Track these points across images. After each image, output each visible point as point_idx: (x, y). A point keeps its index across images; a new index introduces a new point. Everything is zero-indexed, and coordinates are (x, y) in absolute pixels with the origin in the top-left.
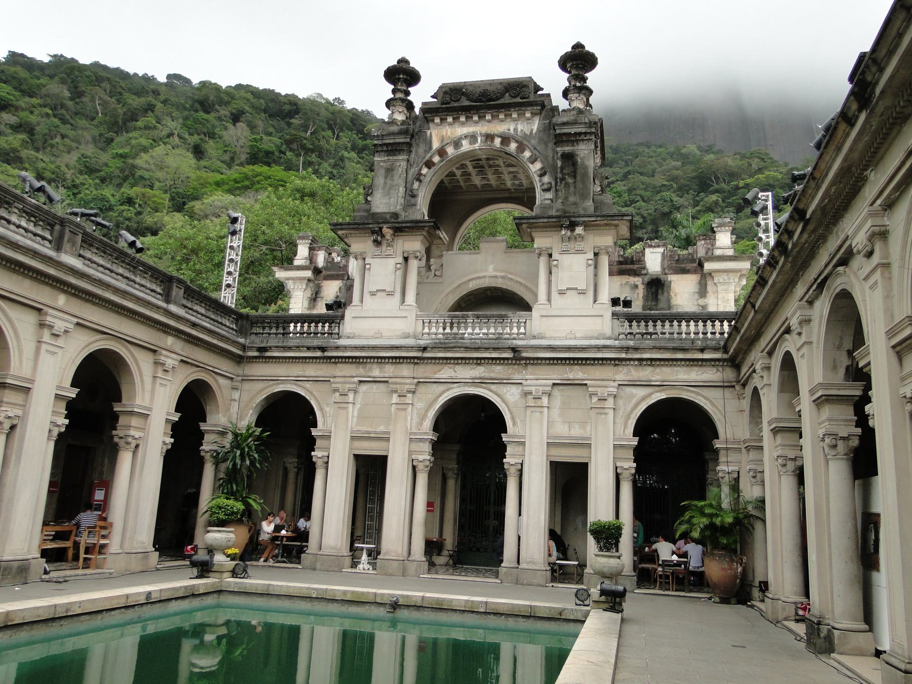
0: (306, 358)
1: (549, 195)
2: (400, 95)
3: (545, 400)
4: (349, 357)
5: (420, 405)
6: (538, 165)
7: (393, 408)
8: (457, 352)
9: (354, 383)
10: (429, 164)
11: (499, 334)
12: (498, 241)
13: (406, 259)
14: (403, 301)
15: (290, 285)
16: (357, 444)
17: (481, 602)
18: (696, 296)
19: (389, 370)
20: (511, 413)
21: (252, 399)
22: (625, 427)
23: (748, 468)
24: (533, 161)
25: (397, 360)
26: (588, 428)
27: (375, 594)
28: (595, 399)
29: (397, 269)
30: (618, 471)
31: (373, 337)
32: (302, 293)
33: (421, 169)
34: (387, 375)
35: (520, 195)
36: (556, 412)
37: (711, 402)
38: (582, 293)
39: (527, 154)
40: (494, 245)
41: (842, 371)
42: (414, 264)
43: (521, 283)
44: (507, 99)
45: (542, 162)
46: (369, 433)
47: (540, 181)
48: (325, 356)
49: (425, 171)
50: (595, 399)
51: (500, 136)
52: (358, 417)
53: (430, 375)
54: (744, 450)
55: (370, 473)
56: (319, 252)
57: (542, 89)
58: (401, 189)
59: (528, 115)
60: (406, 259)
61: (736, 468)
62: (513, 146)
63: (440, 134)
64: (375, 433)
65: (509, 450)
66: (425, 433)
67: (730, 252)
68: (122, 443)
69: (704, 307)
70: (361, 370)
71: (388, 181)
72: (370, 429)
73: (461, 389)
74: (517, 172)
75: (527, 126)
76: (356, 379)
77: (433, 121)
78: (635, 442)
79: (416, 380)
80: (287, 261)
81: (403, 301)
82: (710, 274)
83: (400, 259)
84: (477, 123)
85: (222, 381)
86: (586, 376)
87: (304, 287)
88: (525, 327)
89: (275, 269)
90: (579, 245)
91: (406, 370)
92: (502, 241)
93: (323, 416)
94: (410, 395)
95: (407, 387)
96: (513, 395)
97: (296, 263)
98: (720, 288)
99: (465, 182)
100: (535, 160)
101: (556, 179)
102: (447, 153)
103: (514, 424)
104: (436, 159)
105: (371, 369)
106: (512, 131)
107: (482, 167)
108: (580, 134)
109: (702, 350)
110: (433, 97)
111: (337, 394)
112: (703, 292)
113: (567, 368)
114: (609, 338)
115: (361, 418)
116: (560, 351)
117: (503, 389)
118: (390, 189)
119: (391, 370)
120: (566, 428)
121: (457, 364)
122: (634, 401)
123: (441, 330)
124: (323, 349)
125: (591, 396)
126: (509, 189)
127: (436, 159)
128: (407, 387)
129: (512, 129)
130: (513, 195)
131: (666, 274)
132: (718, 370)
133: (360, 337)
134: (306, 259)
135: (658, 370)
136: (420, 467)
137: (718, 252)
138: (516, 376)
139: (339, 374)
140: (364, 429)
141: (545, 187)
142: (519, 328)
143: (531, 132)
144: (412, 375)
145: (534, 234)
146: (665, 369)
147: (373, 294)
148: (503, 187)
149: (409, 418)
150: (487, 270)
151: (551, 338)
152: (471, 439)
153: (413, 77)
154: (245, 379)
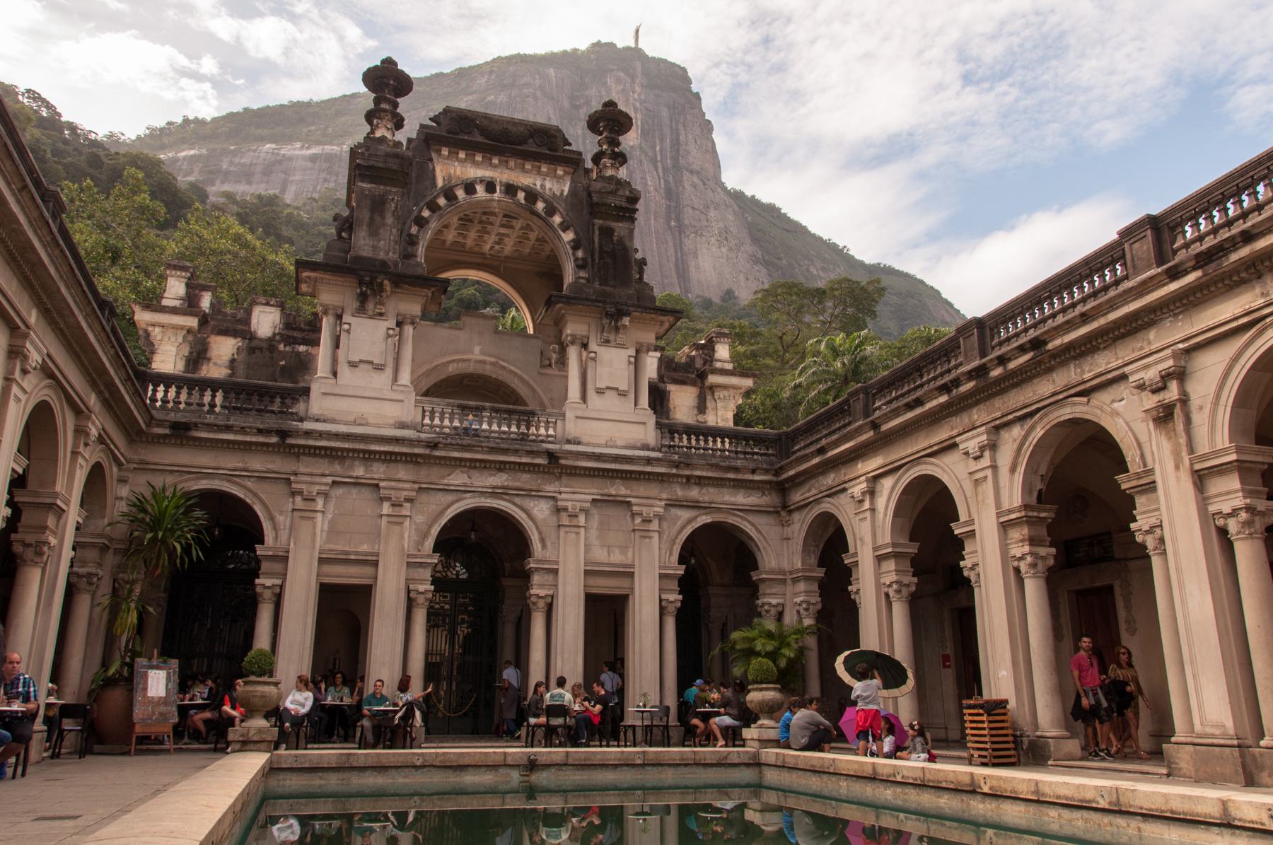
0: (251, 443)
1: (582, 274)
3: (582, 519)
4: (320, 448)
5: (420, 519)
7: (384, 519)
8: (477, 452)
9: (326, 484)
10: (433, 207)
11: (523, 434)
12: (485, 317)
14: (395, 379)
15: (156, 333)
16: (327, 569)
17: (638, 753)
20: (540, 533)
22: (671, 554)
23: (798, 600)
25: (390, 458)
26: (630, 554)
27: (505, 753)
28: (638, 520)
29: (389, 336)
31: (355, 423)
32: (174, 349)
33: (421, 211)
34: (376, 476)
36: (593, 533)
37: (749, 526)
38: (623, 394)
39: (557, 219)
40: (481, 321)
41: (1035, 494)
42: (409, 330)
43: (516, 374)
44: (531, 147)
45: (576, 233)
46: (347, 553)
47: (574, 254)
48: (285, 442)
49: (426, 213)
50: (638, 520)
51: (524, 190)
52: (329, 532)
53: (434, 479)
54: (789, 581)
55: (344, 611)
56: (204, 293)
58: (394, 231)
59: (560, 172)
60: (399, 324)
61: (781, 601)
62: (540, 206)
63: (450, 169)
64: (356, 553)
65: (536, 579)
66: (428, 556)
67: (729, 366)
68: (30, 553)
70: (337, 468)
71: (378, 219)
73: (477, 500)
74: (508, 236)
76: (329, 480)
77: (439, 152)
79: (416, 486)
80: (152, 302)
81: (395, 379)
82: (712, 388)
83: (392, 323)
84: (495, 166)
85: (115, 469)
86: (628, 492)
87: (180, 340)
89: (137, 309)
90: (621, 338)
91: (402, 472)
93: (275, 528)
94: (408, 505)
95: (405, 493)
96: (541, 510)
97: (165, 302)
98: (720, 404)
101: (592, 255)
102: (456, 198)
103: (544, 546)
104: (442, 201)
105: (351, 467)
106: (538, 187)
107: (471, 221)
108: (621, 207)
109: (753, 472)
111: (298, 499)
112: (701, 408)
114: (653, 450)
115: (333, 532)
116: (605, 461)
117: (530, 504)
120: (605, 553)
121: (475, 467)
122: (679, 523)
123: (447, 422)
124: (283, 434)
125: (633, 515)
127: (442, 201)
128: (405, 493)
129: (538, 183)
130: (487, 262)
134: (182, 299)
135: (704, 491)
136: (421, 599)
137: (718, 365)
139: (302, 469)
140: (340, 548)
141: (580, 262)
144: (411, 478)
145: (568, 317)
146: (711, 490)
147: (353, 365)
148: (476, 249)
149: (406, 535)
150: (472, 352)
151: (588, 444)
152: (483, 568)
154: (143, 467)
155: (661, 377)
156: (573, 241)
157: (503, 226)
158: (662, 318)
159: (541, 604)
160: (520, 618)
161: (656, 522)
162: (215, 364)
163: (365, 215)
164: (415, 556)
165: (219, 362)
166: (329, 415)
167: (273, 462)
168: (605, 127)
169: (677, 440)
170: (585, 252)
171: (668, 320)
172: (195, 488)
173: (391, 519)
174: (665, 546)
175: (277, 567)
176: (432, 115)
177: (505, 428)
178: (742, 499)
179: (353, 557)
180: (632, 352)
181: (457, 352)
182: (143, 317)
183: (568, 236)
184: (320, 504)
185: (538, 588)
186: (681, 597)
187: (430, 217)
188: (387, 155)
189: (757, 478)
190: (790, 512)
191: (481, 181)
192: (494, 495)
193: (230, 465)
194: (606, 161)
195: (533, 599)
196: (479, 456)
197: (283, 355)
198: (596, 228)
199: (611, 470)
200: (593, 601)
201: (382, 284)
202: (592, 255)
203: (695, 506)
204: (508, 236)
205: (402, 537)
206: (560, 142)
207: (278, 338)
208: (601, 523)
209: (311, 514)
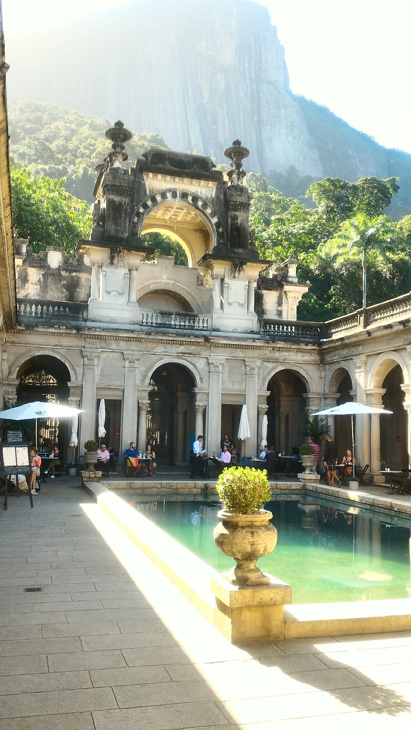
5: (143, 369)
9: (99, 353)
10: (145, 206)
18: (277, 305)
19: (123, 345)
20: (200, 375)
21: (17, 359)
30: (259, 410)
34: (121, 348)
35: (172, 225)
36: (226, 375)
38: (241, 305)
40: (167, 261)
42: (134, 273)
49: (141, 210)
52: (100, 375)
54: (322, 399)
56: (23, 245)
62: (200, 203)
65: (198, 397)
69: (280, 313)
70: (103, 345)
72: (110, 384)
74: (180, 212)
75: (206, 190)
78: (268, 393)
82: (285, 292)
88: (207, 324)
91: (134, 346)
92: (172, 259)
93: (76, 374)
95: (136, 357)
101: (227, 231)
104: (149, 203)
105: (110, 344)
110: (143, 155)
112: (280, 303)
113: (233, 350)
114: (256, 334)
115: (102, 375)
117: (195, 360)
119: (124, 345)
126: (165, 220)
127: (149, 203)
130: (167, 224)
131: (260, 289)
132: (311, 355)
133: (100, 321)
136: (144, 407)
137: (290, 279)
138: (204, 353)
142: (203, 323)
143: (211, 197)
148: (162, 217)
149: (137, 377)
153: (126, 136)
155: (259, 287)
157: (177, 208)
158: (263, 265)
159: (201, 410)
160: (186, 411)
161: (257, 370)
162: (32, 283)
164: (141, 387)
165: (34, 282)
166: (98, 318)
167: (73, 342)
168: (235, 156)
169: (268, 328)
171: (264, 266)
172: (37, 354)
173: (131, 369)
174: (261, 382)
175: (78, 392)
177: (183, 324)
178: (300, 357)
179: (112, 387)
180: (247, 283)
181: (155, 278)
183: (215, 220)
184: (96, 360)
185: (199, 403)
186: (268, 406)
189: (308, 348)
190: (325, 364)
192: (178, 357)
193: (54, 344)
194: (235, 176)
195: (197, 407)
196: (171, 339)
197: (65, 278)
199: (236, 344)
200: (225, 408)
203: (276, 361)
204: (180, 212)
205: (135, 378)
206: (210, 165)
207: (62, 269)
208: (230, 370)
209: (92, 367)
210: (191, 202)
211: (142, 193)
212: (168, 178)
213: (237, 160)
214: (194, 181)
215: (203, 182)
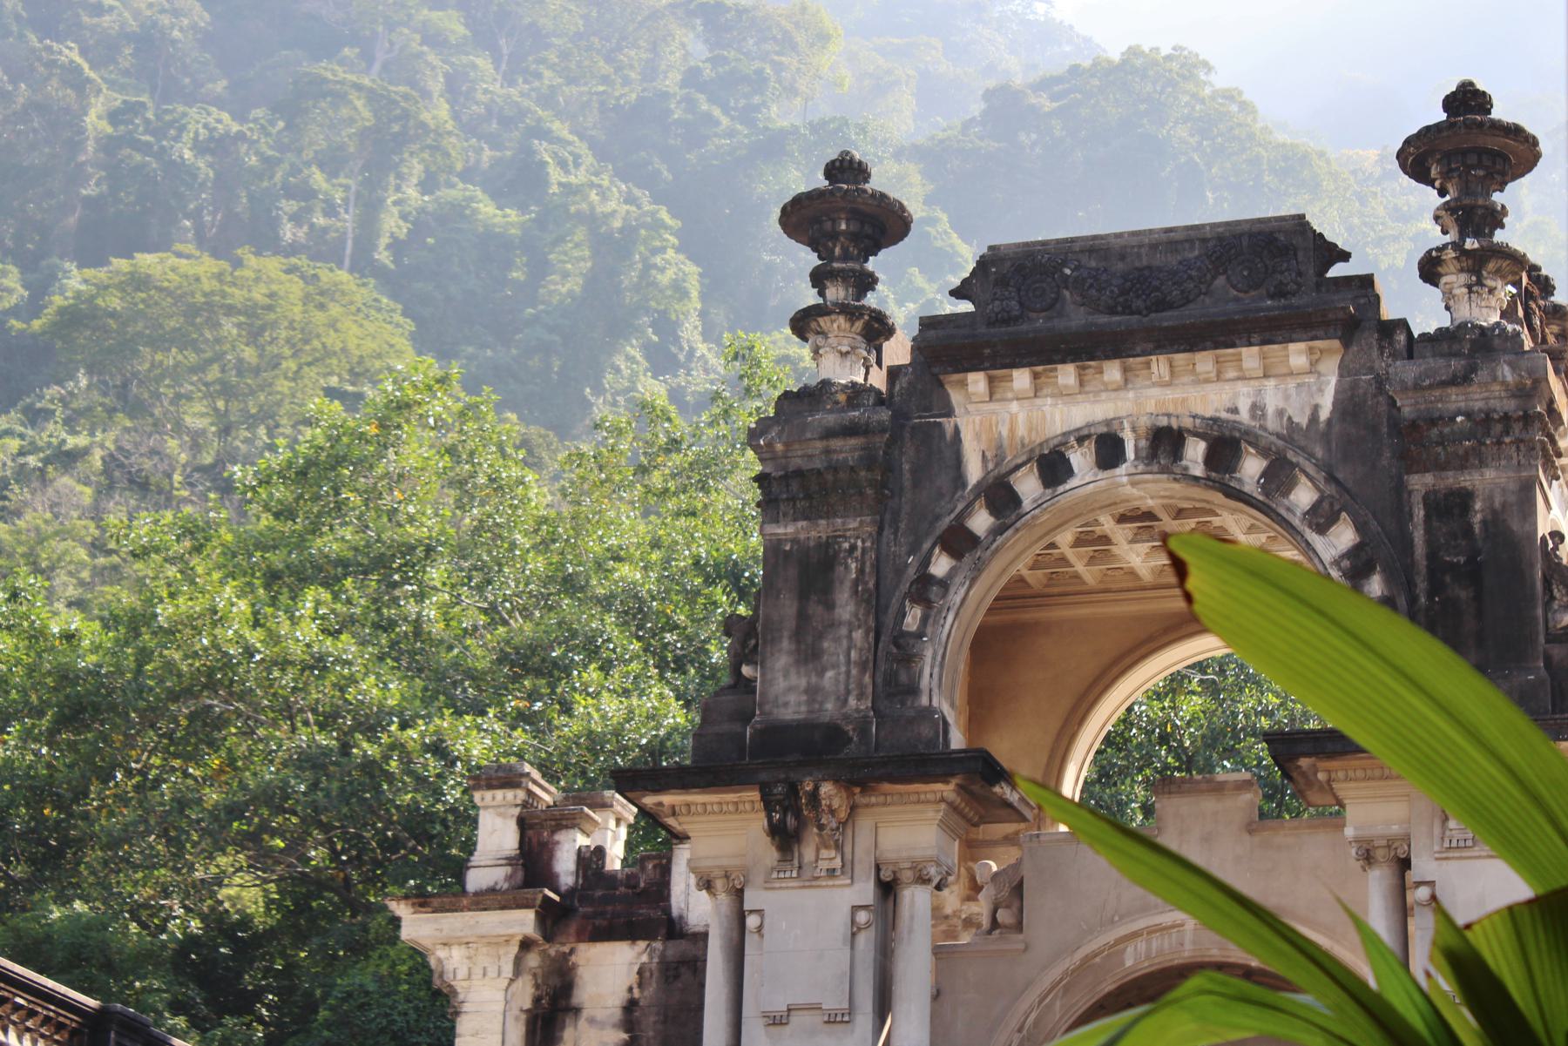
2: (836, 293)
6: (1344, 536)
10: (959, 542)
12: (1219, 789)
13: (888, 889)
15: (453, 963)
24: (1321, 518)
29: (855, 931)
33: (926, 562)
39: (1303, 496)
40: (1209, 804)
45: (1360, 527)
49: (941, 565)
57: (1345, 256)
58: (858, 635)
60: (888, 889)
62: (1252, 468)
71: (816, 610)
80: (443, 881)
83: (865, 891)
87: (508, 969)
89: (401, 909)
97: (478, 879)
99: (1092, 561)
100: (1333, 519)
102: (1015, 500)
104: (981, 521)
118: (820, 636)
127: (981, 521)
134: (510, 861)
145: (1344, 790)
147: (776, 1021)
153: (884, 224)
156: (1353, 553)
163: (788, 607)
165: (600, 1014)
170: (1389, 580)
176: (955, 281)
182: (417, 927)
187: (952, 573)
188: (829, 434)
191: (1081, 440)
198: (1417, 499)
201: (814, 796)
202: (1410, 585)
210: (1198, 470)
211: (944, 481)
212: (1067, 374)
213: (1465, 190)
214: (1204, 361)
215: (1250, 356)
